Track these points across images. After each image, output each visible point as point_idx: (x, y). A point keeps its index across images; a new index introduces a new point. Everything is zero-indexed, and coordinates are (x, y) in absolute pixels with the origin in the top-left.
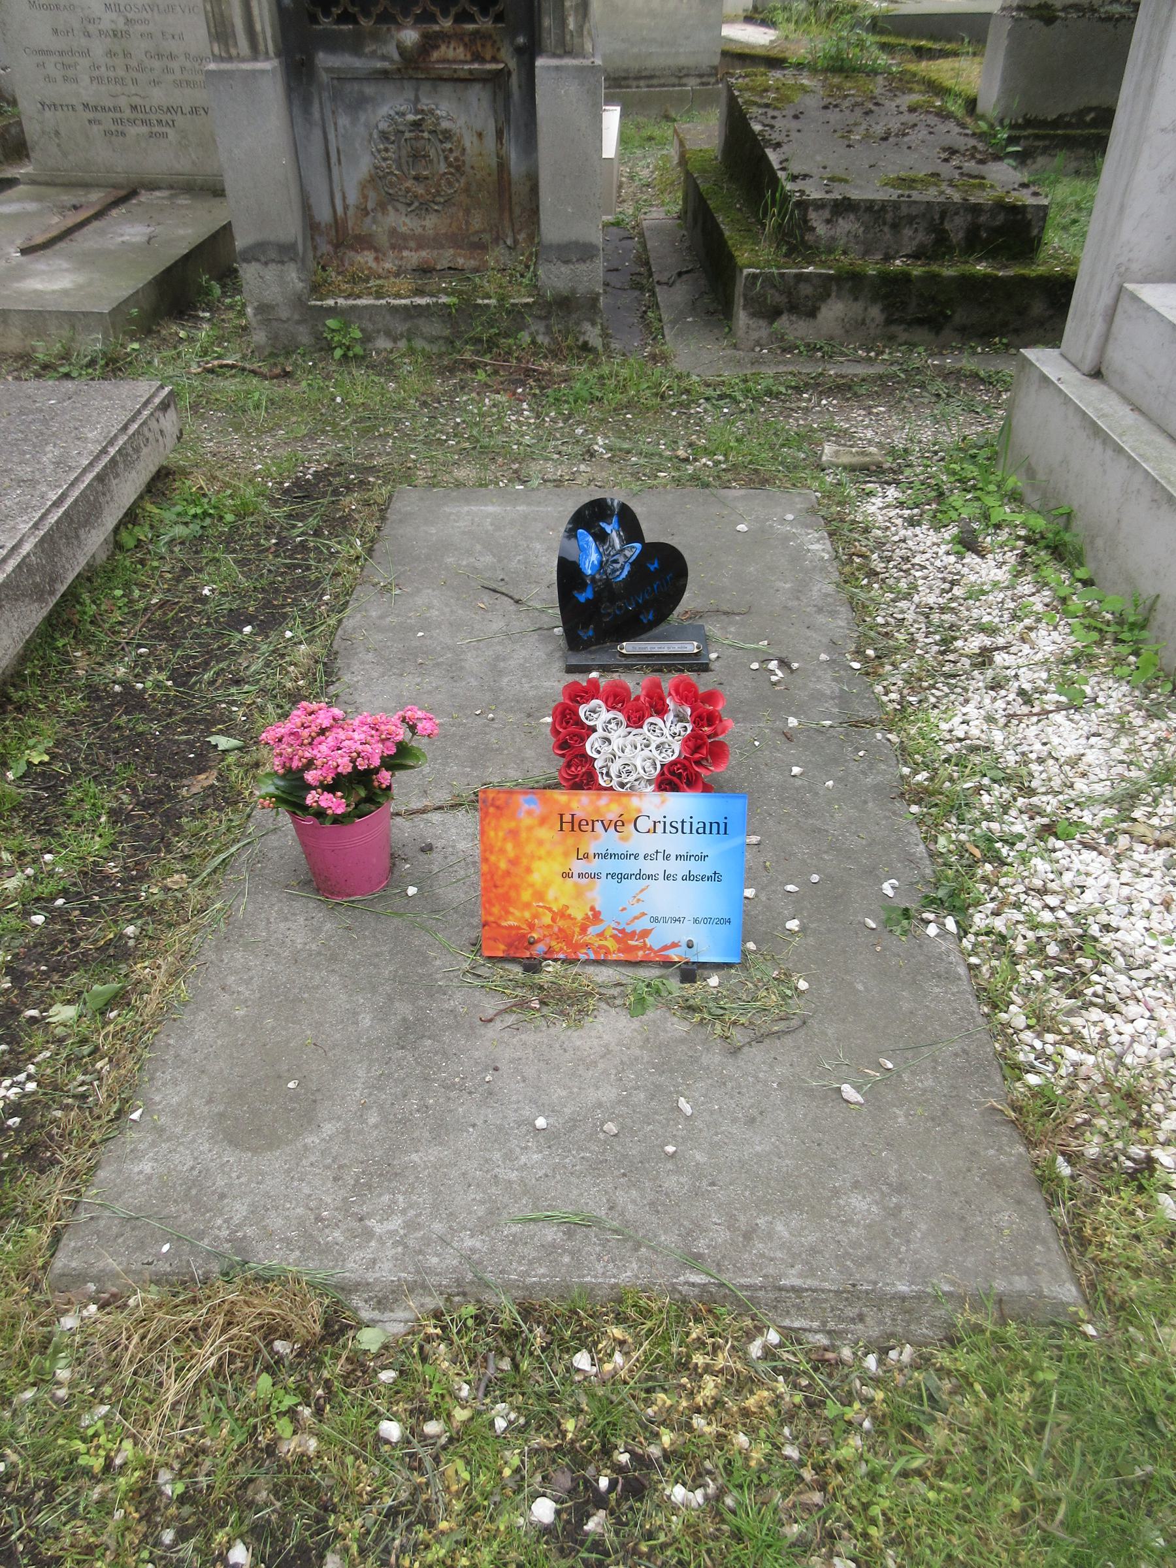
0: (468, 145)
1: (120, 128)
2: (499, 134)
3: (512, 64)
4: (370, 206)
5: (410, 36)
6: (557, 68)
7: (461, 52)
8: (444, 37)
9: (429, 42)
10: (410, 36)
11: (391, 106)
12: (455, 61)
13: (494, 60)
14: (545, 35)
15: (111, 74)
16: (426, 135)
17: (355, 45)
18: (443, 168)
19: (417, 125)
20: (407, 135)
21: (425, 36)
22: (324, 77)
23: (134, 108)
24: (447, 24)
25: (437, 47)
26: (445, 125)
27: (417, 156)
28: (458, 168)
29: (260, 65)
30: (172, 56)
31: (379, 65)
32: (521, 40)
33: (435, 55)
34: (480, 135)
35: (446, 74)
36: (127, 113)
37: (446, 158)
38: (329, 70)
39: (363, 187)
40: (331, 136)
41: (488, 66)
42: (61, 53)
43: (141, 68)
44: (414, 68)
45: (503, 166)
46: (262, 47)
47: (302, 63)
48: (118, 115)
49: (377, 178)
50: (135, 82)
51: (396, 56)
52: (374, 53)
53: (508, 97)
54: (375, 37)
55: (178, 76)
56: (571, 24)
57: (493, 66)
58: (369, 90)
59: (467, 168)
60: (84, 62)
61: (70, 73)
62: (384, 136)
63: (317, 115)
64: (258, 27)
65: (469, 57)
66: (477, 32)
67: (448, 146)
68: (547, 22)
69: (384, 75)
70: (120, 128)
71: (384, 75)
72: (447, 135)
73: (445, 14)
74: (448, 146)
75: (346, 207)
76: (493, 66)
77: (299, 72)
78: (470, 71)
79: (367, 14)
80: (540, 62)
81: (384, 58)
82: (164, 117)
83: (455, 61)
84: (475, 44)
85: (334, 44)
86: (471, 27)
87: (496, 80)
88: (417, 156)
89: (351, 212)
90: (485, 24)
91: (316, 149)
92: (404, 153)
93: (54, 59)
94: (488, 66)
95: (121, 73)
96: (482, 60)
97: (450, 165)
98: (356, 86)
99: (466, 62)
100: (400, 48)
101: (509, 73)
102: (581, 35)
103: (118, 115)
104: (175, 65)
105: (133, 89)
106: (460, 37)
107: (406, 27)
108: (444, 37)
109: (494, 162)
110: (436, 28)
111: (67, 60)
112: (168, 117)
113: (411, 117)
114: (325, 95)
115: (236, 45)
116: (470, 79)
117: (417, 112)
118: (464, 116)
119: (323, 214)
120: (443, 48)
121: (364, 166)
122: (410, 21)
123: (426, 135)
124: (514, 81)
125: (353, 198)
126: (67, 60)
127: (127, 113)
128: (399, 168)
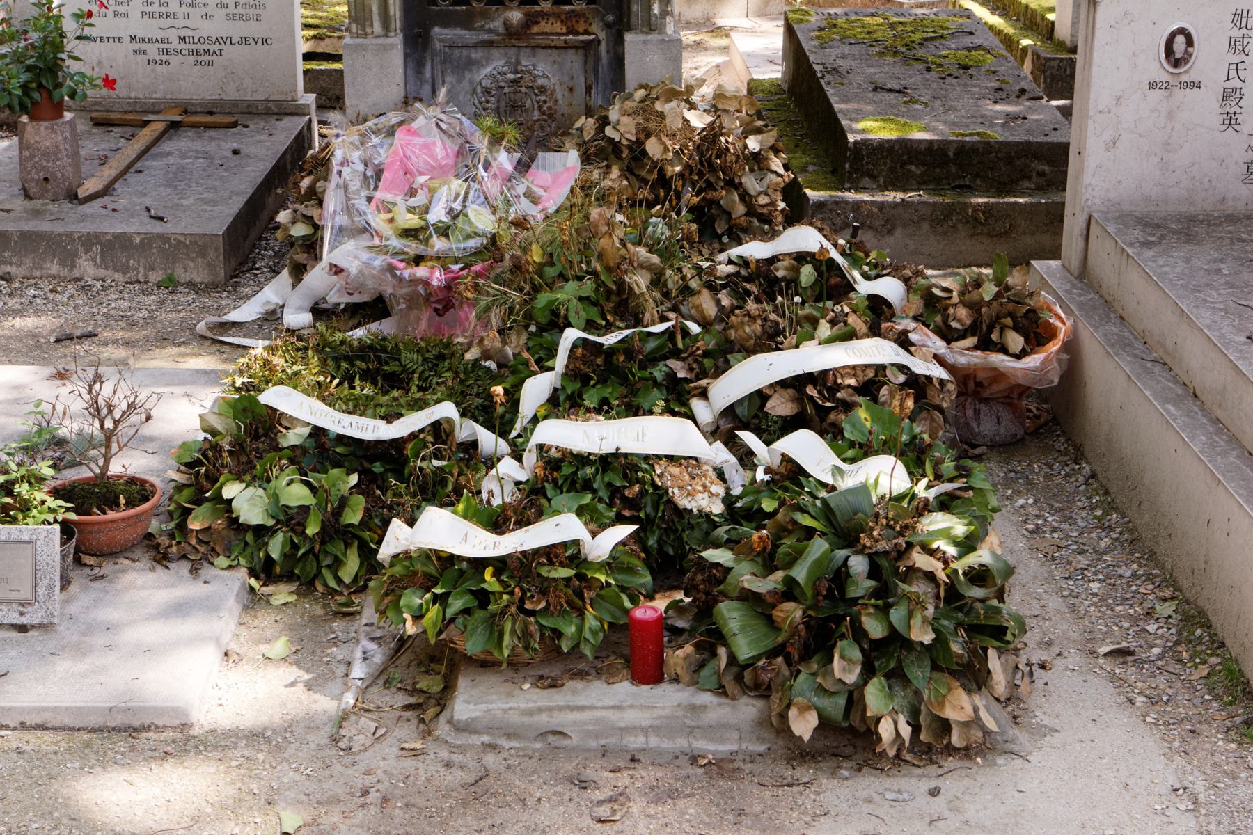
0: (559, 96)
1: (165, 58)
2: (588, 89)
3: (602, 35)
5: (516, 16)
6: (645, 42)
8: (544, 15)
9: (531, 20)
10: (516, 16)
12: (552, 34)
13: (587, 32)
14: (633, 18)
16: (523, 89)
17: (466, 22)
19: (514, 81)
20: (507, 90)
21: (526, 15)
22: (438, 46)
23: (182, 39)
25: (537, 23)
26: (540, 82)
28: (550, 116)
29: (389, 41)
31: (486, 37)
32: (610, 18)
33: (535, 29)
34: (571, 90)
35: (544, 43)
36: (175, 44)
37: (540, 108)
38: (441, 41)
41: (581, 38)
44: (515, 36)
46: (393, 26)
47: (419, 35)
48: (166, 46)
50: (186, 16)
51: (501, 30)
52: (482, 27)
53: (598, 59)
54: (485, 16)
56: (656, 9)
57: (586, 37)
58: (476, 55)
59: (558, 116)
62: (487, 91)
63: (428, 75)
64: (392, 13)
65: (564, 30)
66: (573, 11)
67: (543, 98)
69: (490, 44)
70: (165, 58)
71: (490, 44)
72: (543, 90)
74: (543, 98)
76: (586, 37)
77: (417, 43)
78: (565, 41)
80: (628, 37)
81: (490, 31)
82: (212, 48)
83: (552, 34)
85: (447, 20)
86: (567, 8)
87: (588, 48)
92: (503, 104)
94: (581, 38)
96: (578, 33)
97: (543, 113)
98: (465, 52)
99: (562, 34)
100: (506, 24)
101: (599, 42)
103: (166, 46)
106: (557, 16)
107: (511, 9)
108: (544, 15)
110: (537, 8)
112: (216, 47)
113: (511, 76)
114: (437, 59)
115: (372, 25)
116: (567, 47)
117: (516, 72)
120: (543, 23)
123: (523, 89)
127: (175, 44)
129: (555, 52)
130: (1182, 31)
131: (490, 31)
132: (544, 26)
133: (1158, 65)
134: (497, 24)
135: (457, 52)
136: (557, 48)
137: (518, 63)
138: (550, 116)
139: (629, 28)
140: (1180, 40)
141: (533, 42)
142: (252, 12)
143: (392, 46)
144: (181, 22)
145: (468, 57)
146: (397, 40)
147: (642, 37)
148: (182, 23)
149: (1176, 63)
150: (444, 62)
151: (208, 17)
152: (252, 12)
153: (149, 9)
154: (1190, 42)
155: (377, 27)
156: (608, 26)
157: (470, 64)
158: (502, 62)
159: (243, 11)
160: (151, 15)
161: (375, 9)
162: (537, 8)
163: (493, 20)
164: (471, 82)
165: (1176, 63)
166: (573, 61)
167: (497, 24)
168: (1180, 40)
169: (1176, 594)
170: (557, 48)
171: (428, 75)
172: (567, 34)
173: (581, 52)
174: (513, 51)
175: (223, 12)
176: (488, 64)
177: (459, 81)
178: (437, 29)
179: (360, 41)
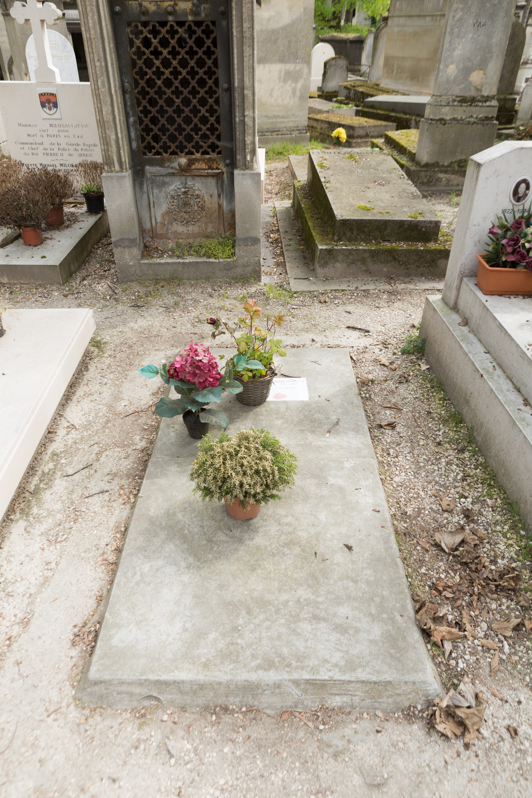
0: (206, 199)
2: (219, 196)
3: (224, 170)
4: (166, 223)
5: (183, 161)
6: (243, 174)
7: (204, 166)
8: (197, 160)
9: (191, 162)
10: (183, 161)
11: (175, 185)
12: (201, 169)
13: (217, 169)
14: (238, 162)
15: (52, 152)
16: (189, 196)
17: (161, 164)
18: (196, 208)
19: (185, 192)
20: (182, 196)
21: (189, 160)
22: (149, 175)
23: (61, 165)
24: (198, 155)
25: (194, 164)
26: (197, 192)
27: (185, 204)
28: (202, 208)
29: (123, 174)
30: (78, 145)
31: (171, 171)
33: (193, 167)
34: (211, 196)
35: (197, 174)
37: (197, 205)
38: (150, 173)
39: (163, 215)
40: (151, 197)
42: (31, 144)
43: (64, 150)
44: (185, 171)
45: (220, 206)
46: (124, 167)
49: (168, 212)
50: (62, 155)
51: (178, 167)
52: (169, 166)
53: (223, 182)
54: (169, 160)
55: (80, 152)
56: (248, 158)
57: (217, 171)
58: (167, 179)
60: (41, 147)
61: (35, 152)
62: (173, 197)
63: (145, 189)
64: (123, 160)
65: (207, 167)
66: (210, 158)
67: (198, 200)
68: (238, 157)
69: (173, 174)
71: (173, 174)
72: (198, 196)
73: (198, 152)
74: (198, 200)
75: (156, 223)
76: (217, 171)
77: (138, 174)
78: (208, 173)
79: (166, 152)
80: (236, 172)
81: (172, 168)
83: (201, 169)
84: (210, 163)
85: (152, 163)
86: (208, 156)
87: (218, 176)
88: (185, 204)
89: (158, 225)
90: (213, 155)
91: (145, 202)
92: (180, 203)
93: (29, 146)
95: (56, 151)
96: (213, 169)
97: (199, 207)
98: (161, 178)
99: (206, 169)
101: (223, 173)
102: (253, 162)
104: (79, 148)
105: (62, 158)
106: (203, 160)
107: (182, 157)
108: (197, 160)
109: (217, 206)
111: (34, 146)
113: (183, 190)
114: (149, 182)
115: (114, 167)
117: (186, 188)
118: (205, 189)
119: (148, 226)
120: (197, 164)
121: (164, 208)
122: (183, 154)
123: (189, 196)
124: (225, 176)
125: (159, 219)
126: (34, 146)
128: (179, 208)
129: (203, 178)
130: (525, 181)
131: (172, 168)
132: (197, 165)
133: (508, 200)
134: (175, 165)
135: (158, 178)
136: (204, 176)
137: (186, 183)
138: (202, 208)
139: (236, 168)
140: (523, 186)
141: (193, 174)
142: (88, 153)
143: (124, 177)
144: (60, 157)
145: (163, 181)
146: (128, 174)
147: (242, 172)
148: (62, 158)
149: (518, 200)
150: (152, 183)
151: (70, 155)
152: (88, 153)
153: (46, 152)
154: (528, 188)
155: (117, 167)
156: (227, 165)
157: (164, 184)
158: (179, 183)
159: (85, 153)
160: (47, 154)
161: (115, 158)
162: (194, 157)
163: (173, 162)
164: (165, 193)
165: (518, 200)
166: (212, 182)
167: (175, 165)
168: (523, 186)
169: (502, 489)
170: (204, 176)
171: (145, 189)
172: (208, 169)
173: (215, 178)
174: (183, 178)
175: (77, 152)
176: (172, 184)
177: (160, 192)
178: (147, 167)
179: (109, 174)
